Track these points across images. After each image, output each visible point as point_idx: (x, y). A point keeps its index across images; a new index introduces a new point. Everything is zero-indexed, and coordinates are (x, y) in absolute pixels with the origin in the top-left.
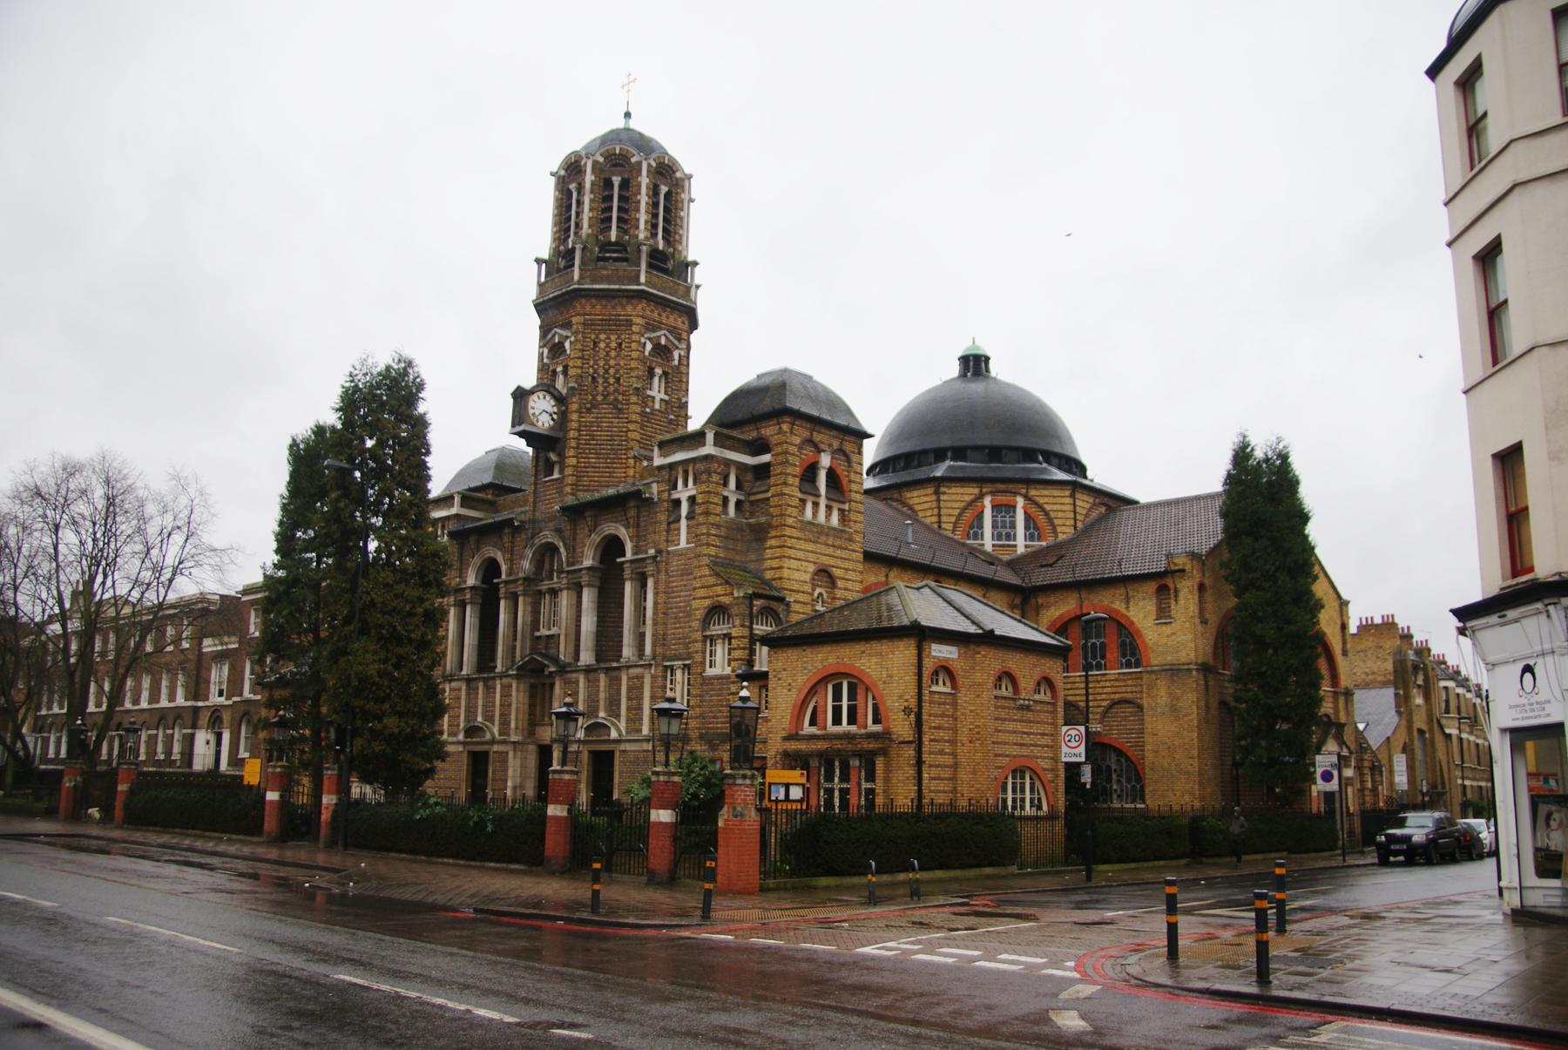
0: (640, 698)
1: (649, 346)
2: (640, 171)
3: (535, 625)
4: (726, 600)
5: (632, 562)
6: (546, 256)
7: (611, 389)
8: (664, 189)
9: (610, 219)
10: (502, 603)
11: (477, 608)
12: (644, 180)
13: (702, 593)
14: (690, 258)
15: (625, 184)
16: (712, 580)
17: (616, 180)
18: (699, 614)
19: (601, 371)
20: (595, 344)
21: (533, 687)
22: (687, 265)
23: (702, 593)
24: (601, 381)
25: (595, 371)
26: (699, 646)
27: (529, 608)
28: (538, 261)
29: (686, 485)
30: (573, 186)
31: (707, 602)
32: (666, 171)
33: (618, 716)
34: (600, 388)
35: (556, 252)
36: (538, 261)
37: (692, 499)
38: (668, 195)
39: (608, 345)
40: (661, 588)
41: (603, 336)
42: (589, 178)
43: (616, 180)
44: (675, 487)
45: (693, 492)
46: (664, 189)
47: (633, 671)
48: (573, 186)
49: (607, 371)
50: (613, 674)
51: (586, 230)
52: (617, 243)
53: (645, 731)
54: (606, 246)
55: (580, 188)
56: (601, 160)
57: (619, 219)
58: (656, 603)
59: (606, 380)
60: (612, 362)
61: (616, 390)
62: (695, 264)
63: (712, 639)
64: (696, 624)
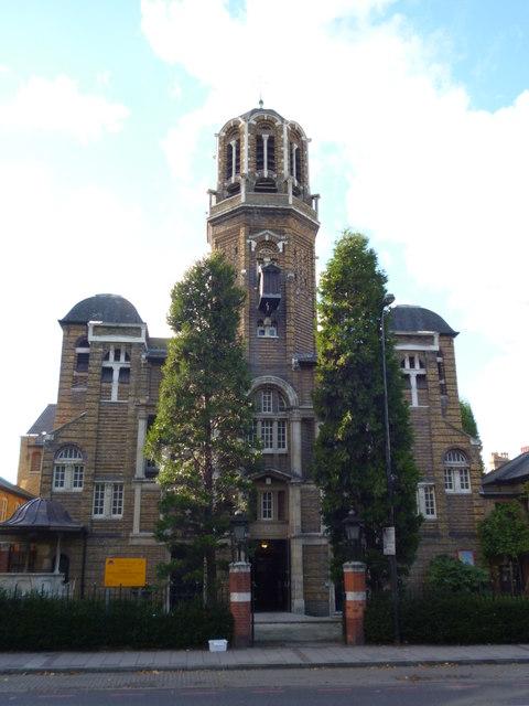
2: (282, 132)
4: (464, 446)
6: (215, 188)
8: (296, 146)
9: (262, 163)
12: (285, 137)
13: (441, 438)
14: (312, 192)
15: (271, 140)
16: (450, 432)
17: (265, 137)
22: (313, 197)
23: (441, 438)
28: (211, 192)
29: (412, 365)
30: (233, 143)
31: (447, 446)
32: (296, 133)
35: (221, 187)
36: (211, 192)
38: (297, 150)
42: (245, 137)
43: (265, 137)
45: (422, 372)
46: (296, 146)
48: (233, 143)
51: (245, 170)
52: (268, 180)
54: (262, 179)
55: (238, 147)
56: (255, 123)
57: (269, 163)
62: (317, 196)
63: (450, 470)
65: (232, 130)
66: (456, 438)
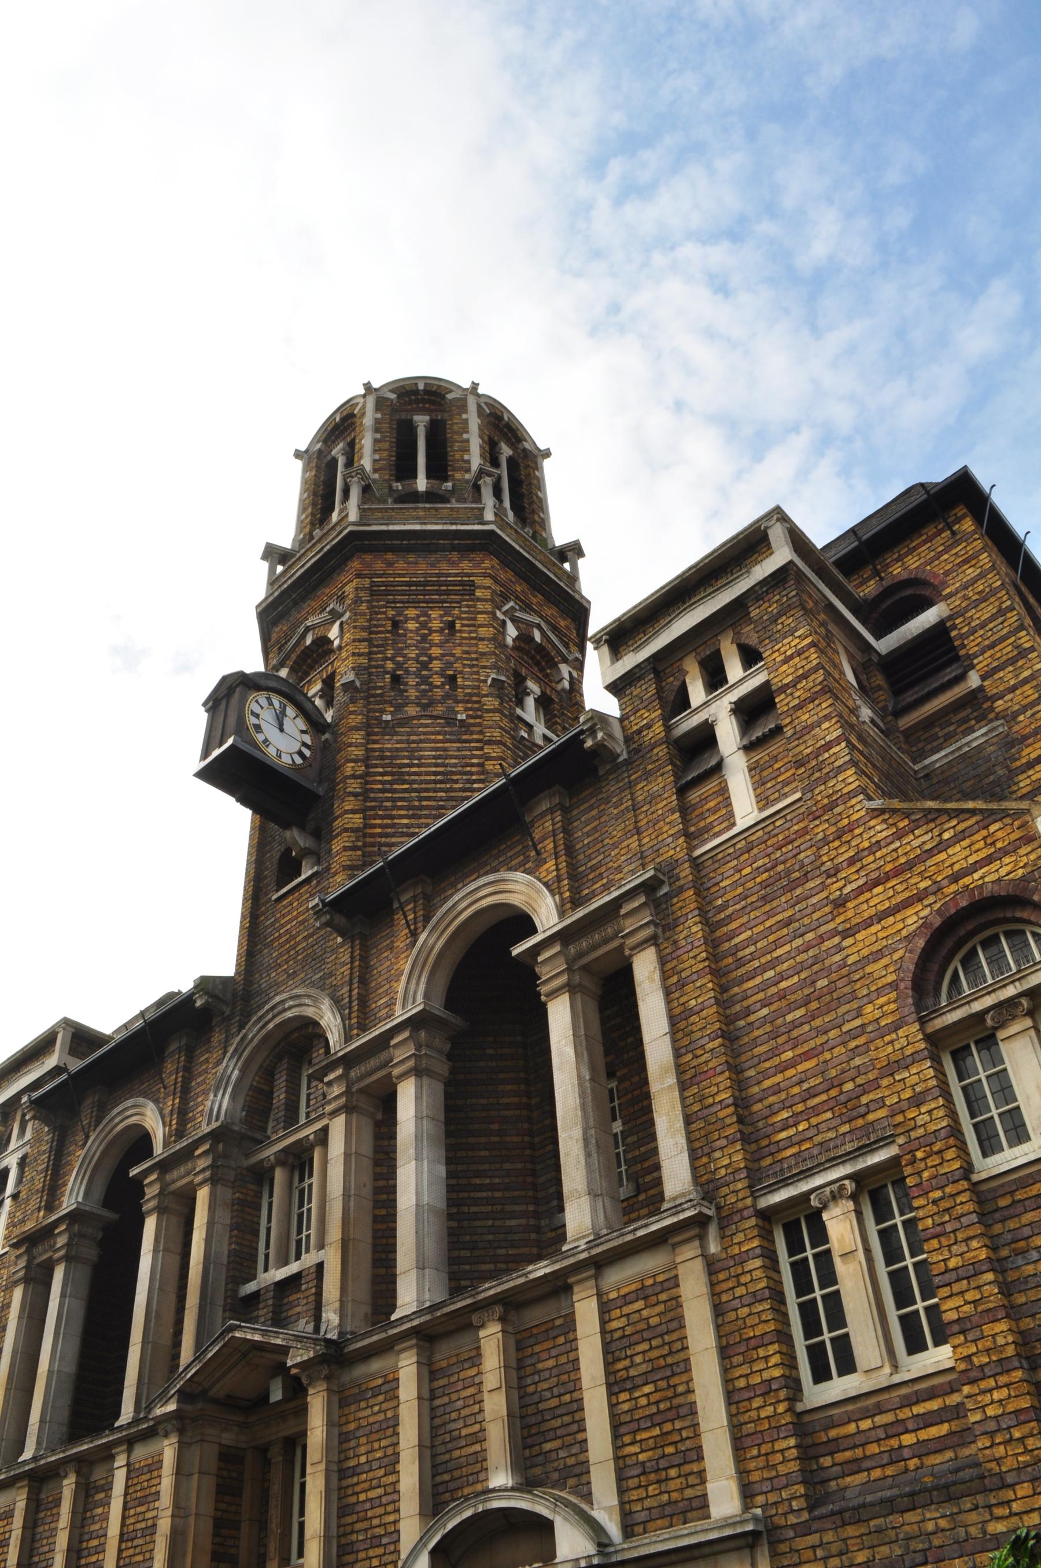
0: (675, 1366)
1: (512, 632)
3: (242, 1261)
5: (564, 936)
7: (439, 692)
10: (150, 1225)
11: (84, 1274)
18: (892, 968)
19: (413, 666)
20: (396, 625)
21: (228, 1457)
24: (412, 681)
25: (399, 666)
26: (921, 1074)
27: (225, 1217)
31: (912, 919)
33: (575, 1477)
34: (413, 693)
37: (753, 710)
39: (424, 625)
40: (694, 959)
41: (412, 613)
44: (682, 702)
47: (620, 1277)
49: (425, 666)
50: (536, 1324)
53: (724, 1500)
58: (677, 1021)
59: (425, 680)
60: (436, 651)
61: (447, 697)
64: (881, 1009)
65: (341, 426)
66: (958, 855)
